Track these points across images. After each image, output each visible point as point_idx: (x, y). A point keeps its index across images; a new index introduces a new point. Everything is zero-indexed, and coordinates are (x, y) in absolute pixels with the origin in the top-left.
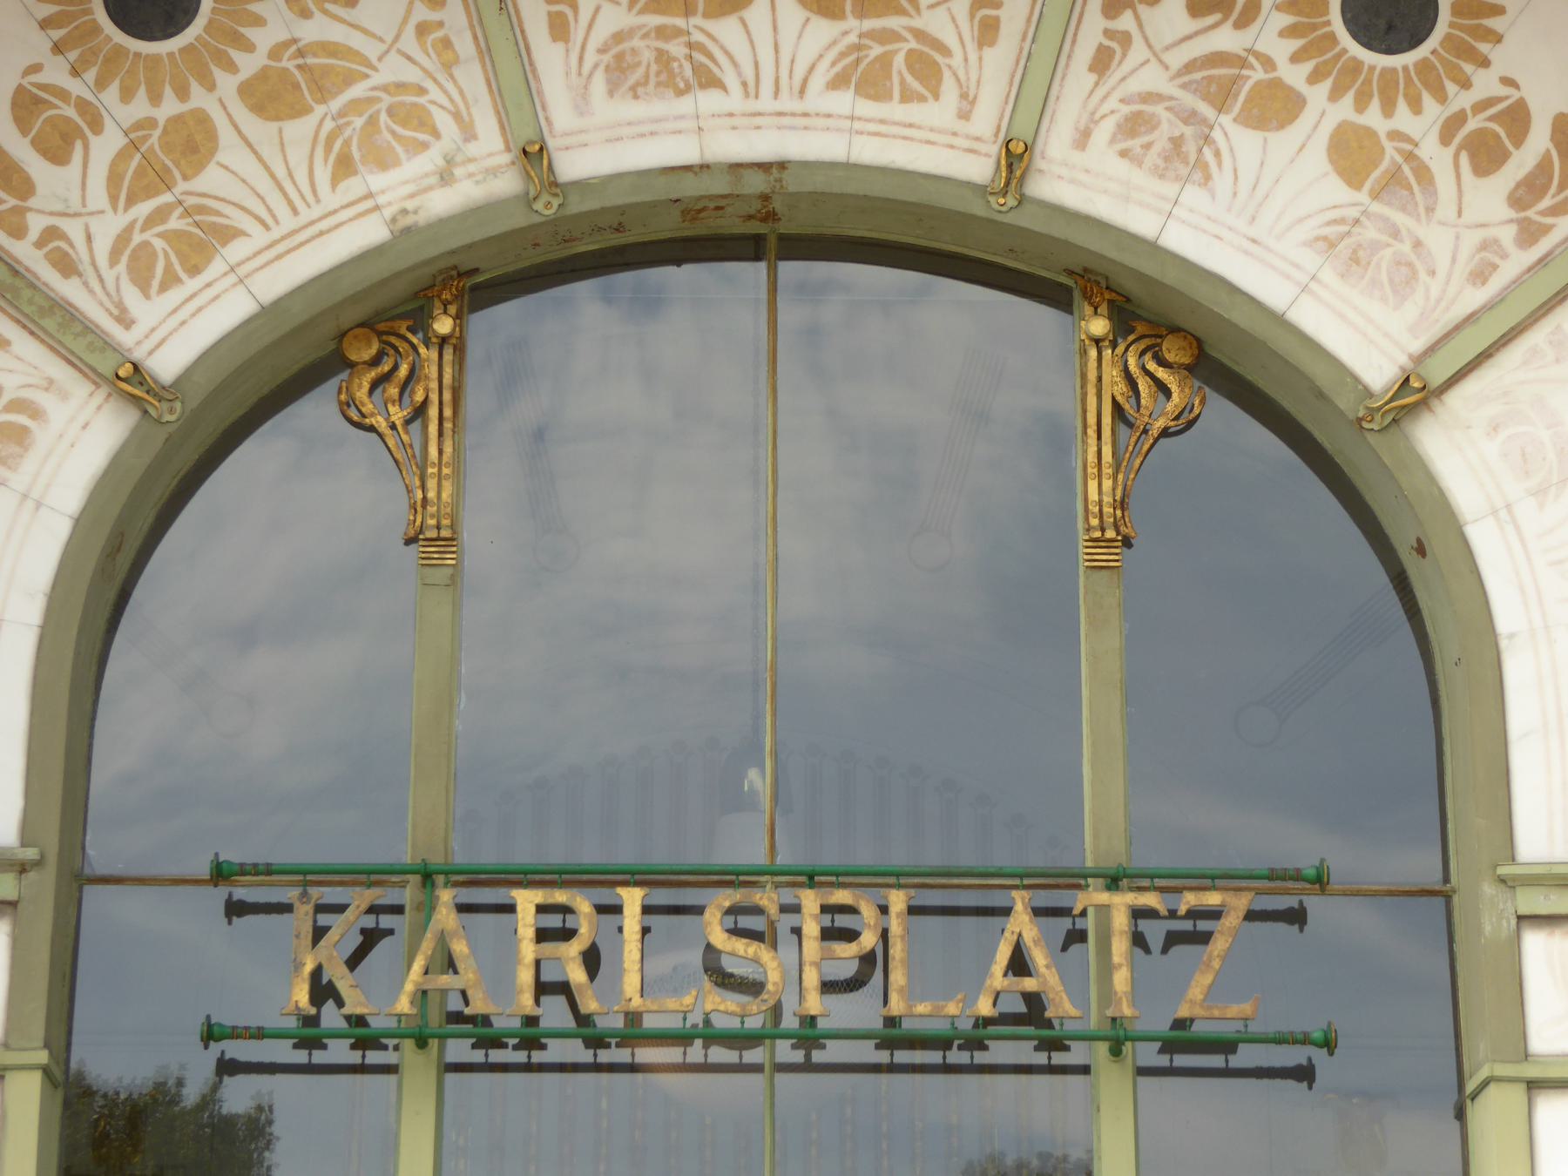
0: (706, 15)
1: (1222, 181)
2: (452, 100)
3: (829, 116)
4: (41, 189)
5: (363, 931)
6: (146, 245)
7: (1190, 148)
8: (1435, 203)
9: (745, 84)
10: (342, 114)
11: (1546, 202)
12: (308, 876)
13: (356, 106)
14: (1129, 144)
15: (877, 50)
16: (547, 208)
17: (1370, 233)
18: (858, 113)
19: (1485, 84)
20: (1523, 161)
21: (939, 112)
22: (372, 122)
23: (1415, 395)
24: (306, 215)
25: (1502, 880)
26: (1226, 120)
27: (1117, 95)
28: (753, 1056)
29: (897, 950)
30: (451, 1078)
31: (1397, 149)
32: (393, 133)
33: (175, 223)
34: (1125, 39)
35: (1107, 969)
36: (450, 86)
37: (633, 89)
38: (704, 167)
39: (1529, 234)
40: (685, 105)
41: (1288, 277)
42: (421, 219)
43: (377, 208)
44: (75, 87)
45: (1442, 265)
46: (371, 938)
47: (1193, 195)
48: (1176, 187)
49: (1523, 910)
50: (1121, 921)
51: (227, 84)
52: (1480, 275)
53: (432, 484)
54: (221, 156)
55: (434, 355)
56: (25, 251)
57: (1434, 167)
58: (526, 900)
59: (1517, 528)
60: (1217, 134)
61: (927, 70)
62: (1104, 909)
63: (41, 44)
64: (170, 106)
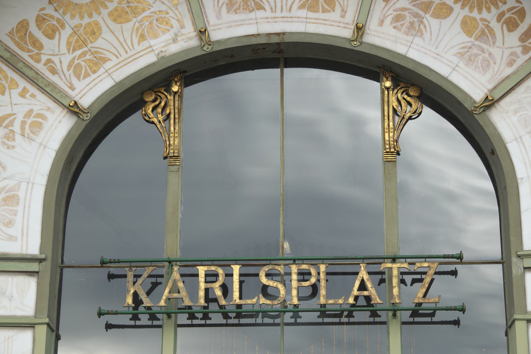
1: (427, 36)
2: (177, 16)
3: (299, 18)
4: (45, 47)
5: (152, 283)
6: (79, 64)
7: (416, 25)
8: (496, 41)
9: (271, 8)
10: (141, 21)
12: (131, 263)
14: (396, 24)
16: (208, 49)
17: (475, 51)
18: (308, 16)
21: (335, 15)
22: (151, 23)
23: (489, 103)
24: (130, 53)
25: (519, 256)
26: (428, 16)
27: (393, 8)
28: (277, 321)
29: (323, 283)
30: (179, 329)
31: (483, 24)
32: (158, 26)
33: (88, 57)
35: (391, 287)
36: (176, 11)
37: (235, 11)
38: (258, 35)
40: (252, 15)
41: (449, 66)
42: (167, 54)
43: (153, 50)
44: (56, 15)
45: (498, 61)
46: (155, 285)
47: (417, 40)
48: (412, 37)
49: (526, 266)
50: (395, 272)
52: (510, 64)
53: (172, 139)
54: (103, 35)
55: (172, 98)
56: (40, 67)
57: (495, 29)
58: (202, 270)
59: (523, 144)
60: (425, 20)
62: (391, 269)
64: (86, 20)
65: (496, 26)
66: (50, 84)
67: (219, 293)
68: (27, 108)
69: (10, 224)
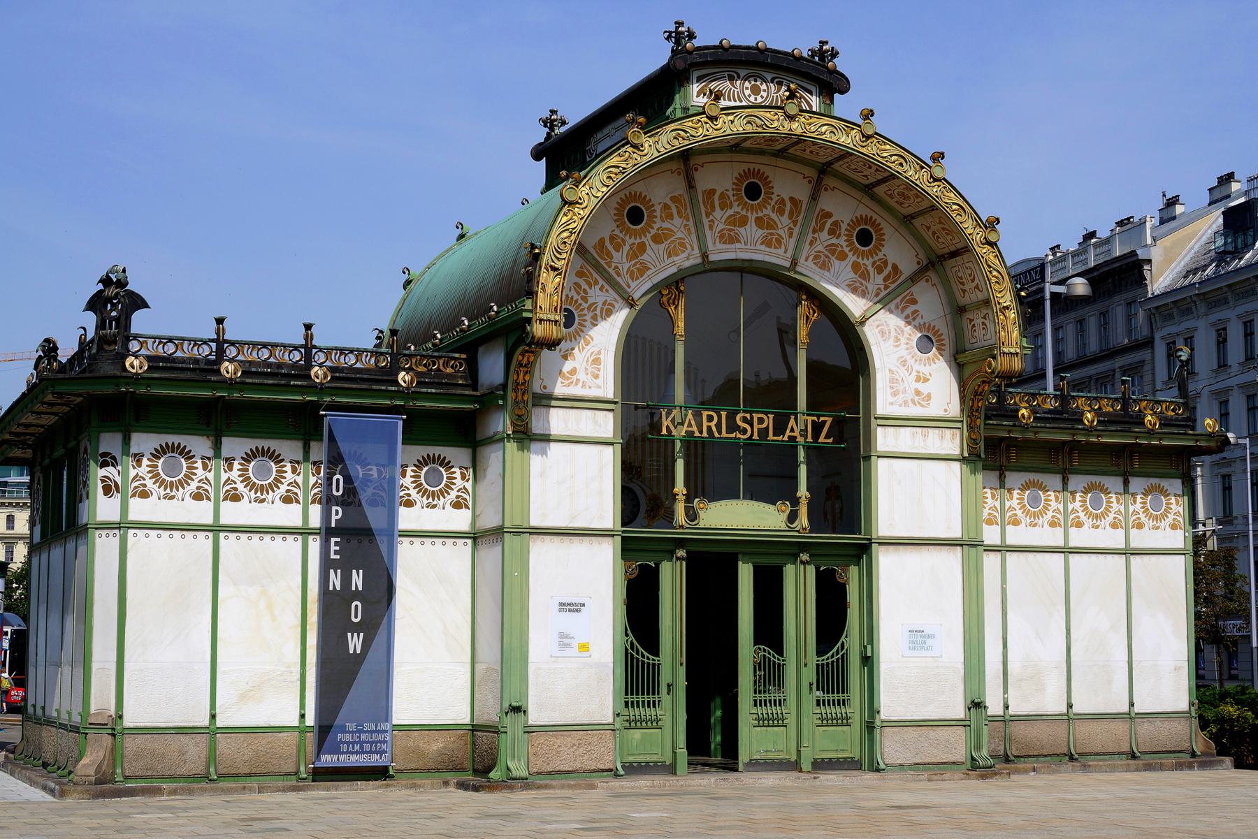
19: (880, 255)
20: (886, 272)
21: (781, 251)
39: (886, 287)
47: (826, 273)
51: (649, 236)
56: (610, 270)
58: (705, 413)
61: (779, 242)
63: (614, 226)
64: (638, 241)
65: (871, 269)
66: (618, 283)
67: (714, 429)
69: (596, 377)
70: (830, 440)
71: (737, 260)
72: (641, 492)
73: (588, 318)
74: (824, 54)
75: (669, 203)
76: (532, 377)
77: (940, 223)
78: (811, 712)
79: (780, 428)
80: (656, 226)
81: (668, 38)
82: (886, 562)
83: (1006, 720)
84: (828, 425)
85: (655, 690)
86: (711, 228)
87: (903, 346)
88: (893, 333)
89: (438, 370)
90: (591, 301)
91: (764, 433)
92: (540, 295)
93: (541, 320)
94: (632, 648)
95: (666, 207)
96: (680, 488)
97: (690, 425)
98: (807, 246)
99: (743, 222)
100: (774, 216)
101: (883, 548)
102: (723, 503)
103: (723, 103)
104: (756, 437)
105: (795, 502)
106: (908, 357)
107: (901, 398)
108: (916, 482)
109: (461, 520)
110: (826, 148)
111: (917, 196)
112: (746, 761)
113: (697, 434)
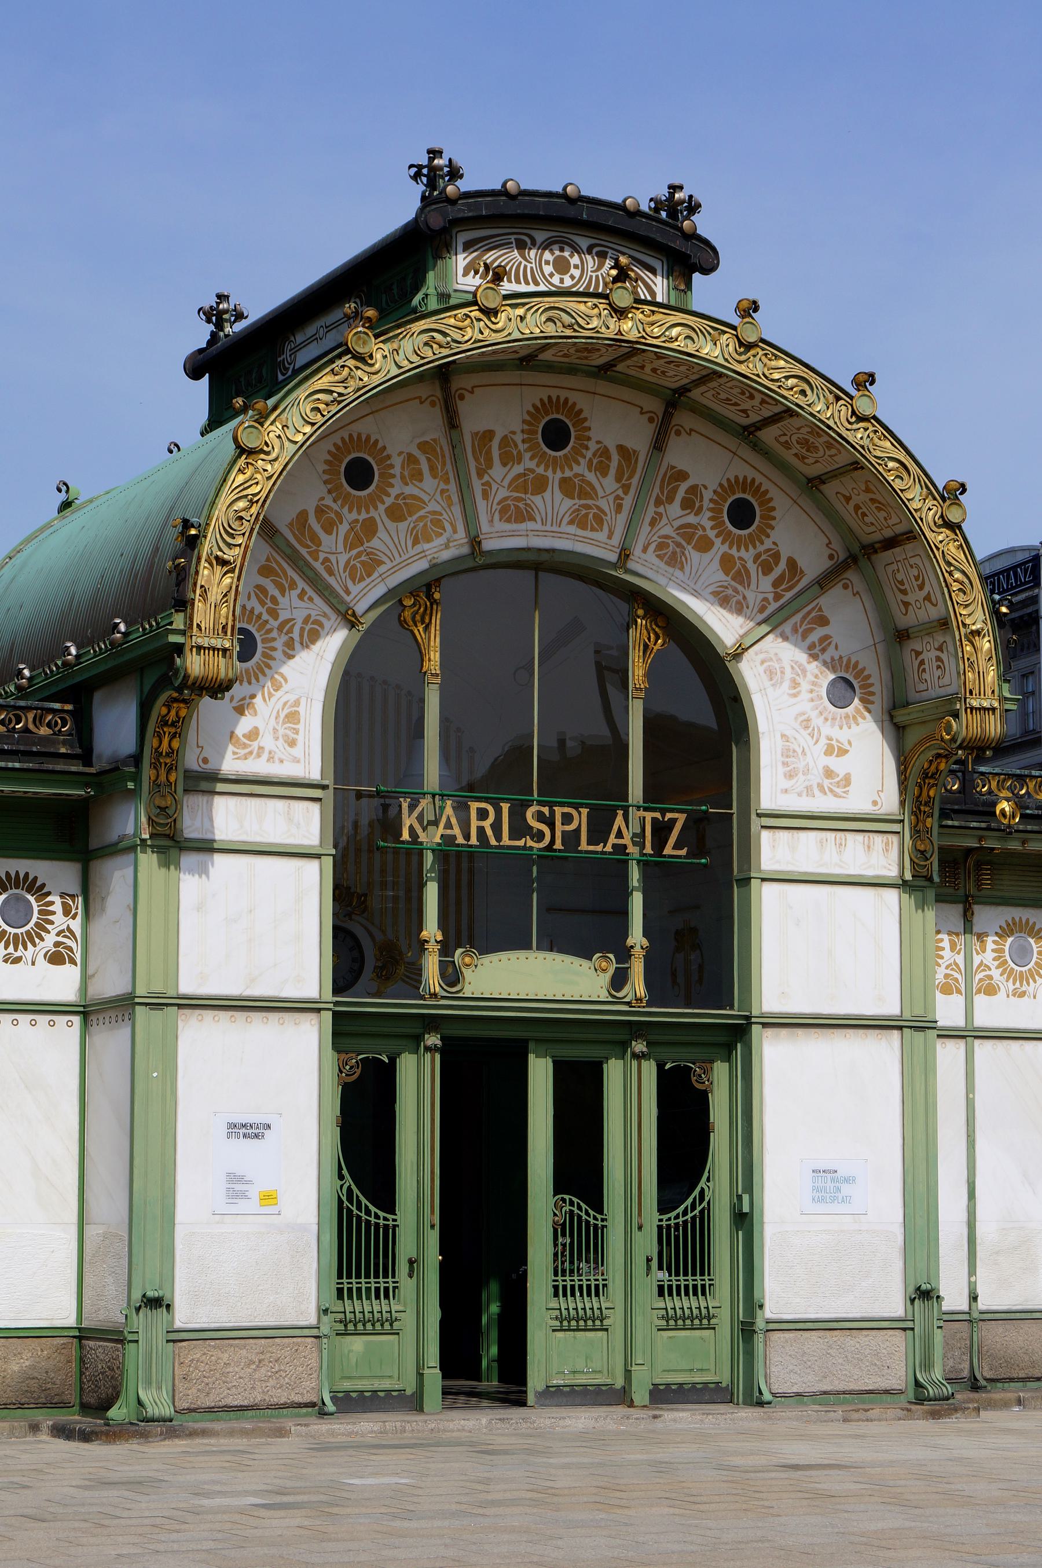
0: (532, 494)
1: (687, 569)
10: (416, 521)
11: (783, 587)
13: (421, 518)
15: (584, 512)
17: (730, 592)
19: (768, 544)
20: (777, 571)
21: (602, 536)
24: (404, 557)
26: (690, 547)
33: (363, 558)
34: (660, 515)
39: (777, 597)
40: (523, 526)
42: (439, 561)
47: (678, 573)
51: (382, 508)
53: (432, 653)
56: (318, 566)
58: (474, 806)
60: (686, 552)
61: (599, 520)
63: (323, 490)
64: (364, 516)
65: (752, 567)
66: (329, 587)
67: (489, 832)
68: (306, 612)
69: (292, 743)
70: (683, 852)
71: (528, 549)
72: (366, 937)
73: (279, 644)
74: (676, 208)
75: (417, 453)
76: (184, 743)
77: (868, 490)
78: (649, 1305)
79: (599, 831)
80: (394, 492)
81: (416, 177)
82: (775, 1056)
83: (973, 1319)
84: (678, 826)
85: (388, 1269)
86: (485, 495)
87: (805, 696)
88: (789, 674)
89: (26, 730)
90: (283, 615)
91: (572, 839)
92: (199, 605)
93: (199, 648)
94: (350, 1198)
95: (411, 459)
96: (431, 930)
97: (449, 825)
98: (646, 528)
99: (540, 485)
100: (591, 477)
101: (769, 1032)
102: (504, 956)
103: (508, 286)
104: (558, 845)
105: (624, 954)
106: (813, 714)
107: (800, 782)
108: (825, 922)
109: (63, 984)
110: (678, 363)
111: (829, 446)
112: (541, 1387)
113: (460, 840)
